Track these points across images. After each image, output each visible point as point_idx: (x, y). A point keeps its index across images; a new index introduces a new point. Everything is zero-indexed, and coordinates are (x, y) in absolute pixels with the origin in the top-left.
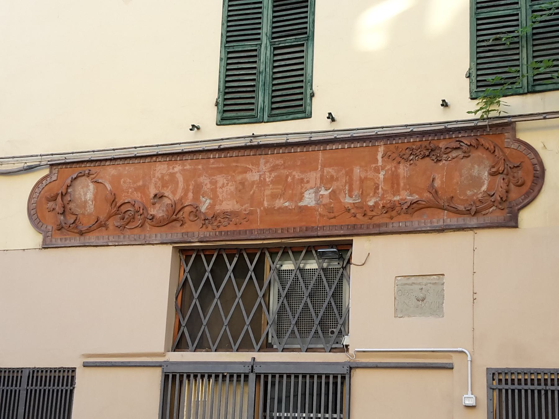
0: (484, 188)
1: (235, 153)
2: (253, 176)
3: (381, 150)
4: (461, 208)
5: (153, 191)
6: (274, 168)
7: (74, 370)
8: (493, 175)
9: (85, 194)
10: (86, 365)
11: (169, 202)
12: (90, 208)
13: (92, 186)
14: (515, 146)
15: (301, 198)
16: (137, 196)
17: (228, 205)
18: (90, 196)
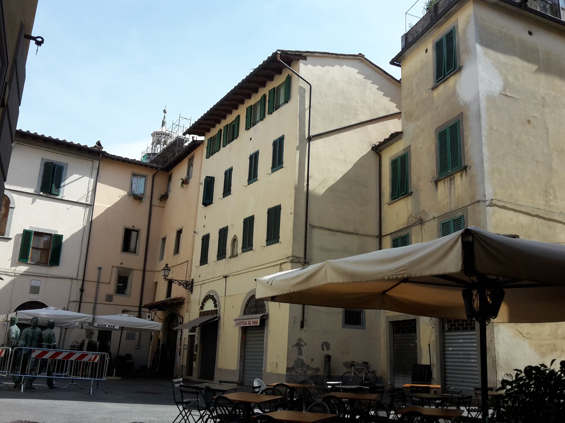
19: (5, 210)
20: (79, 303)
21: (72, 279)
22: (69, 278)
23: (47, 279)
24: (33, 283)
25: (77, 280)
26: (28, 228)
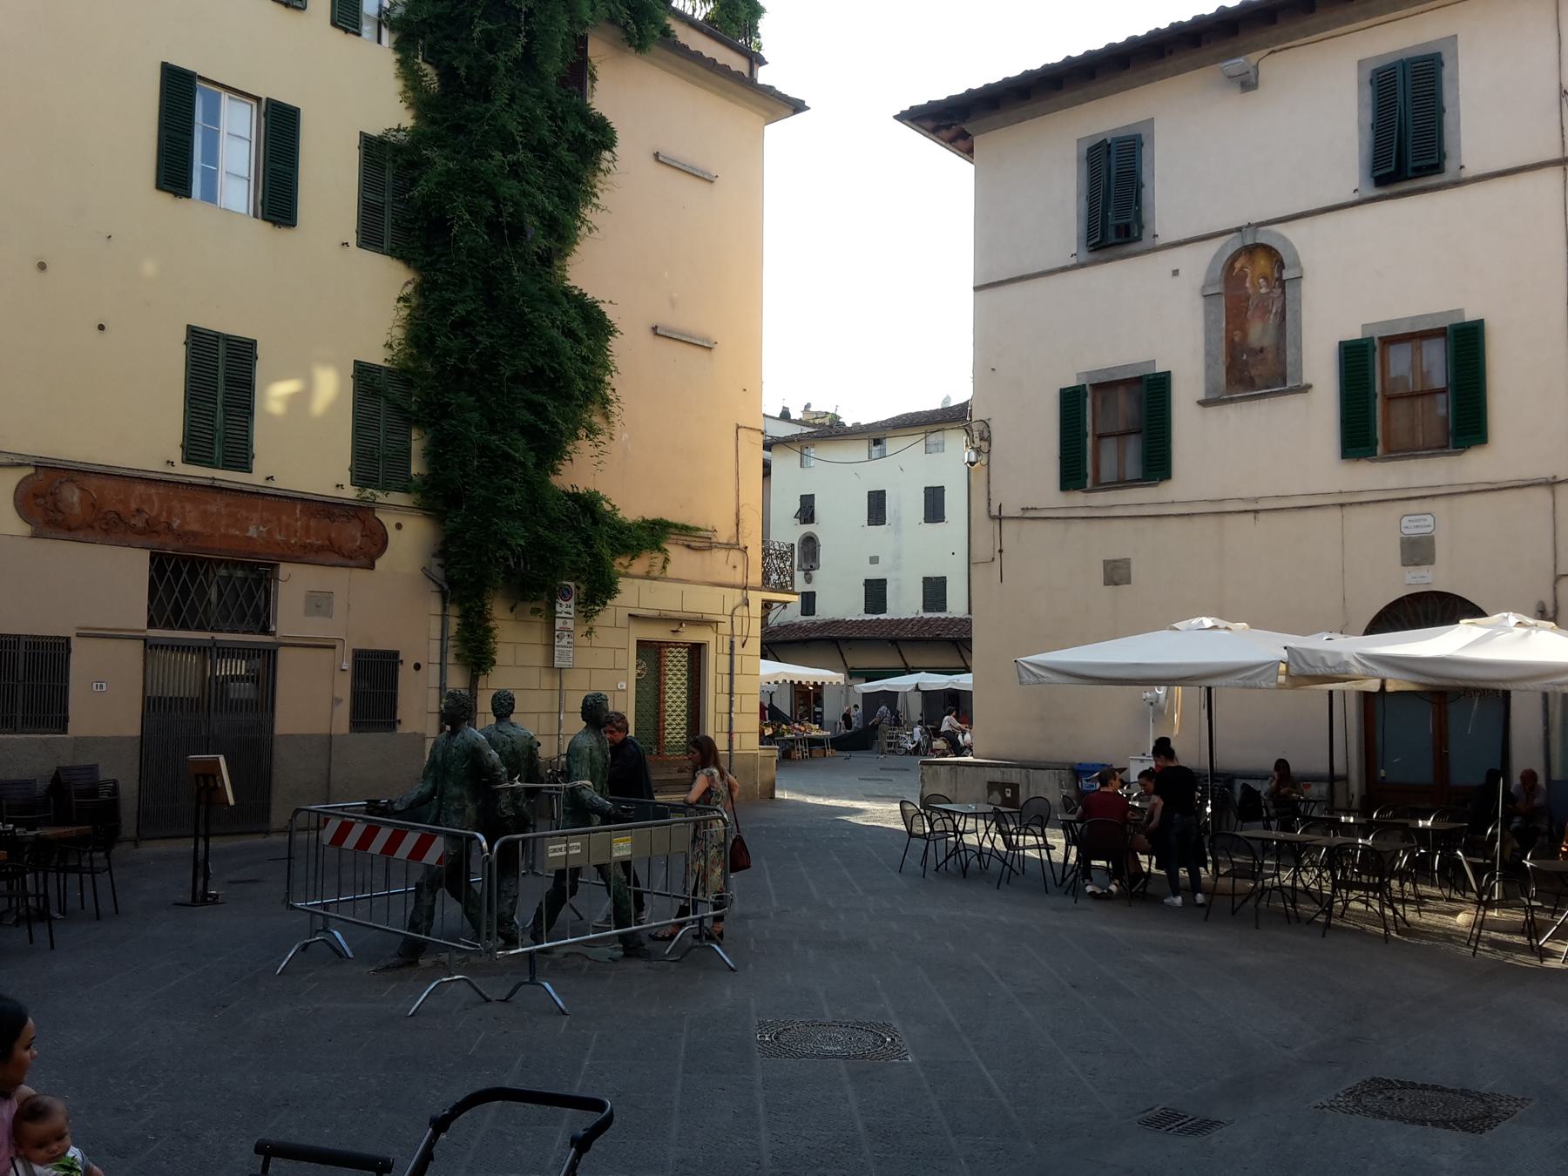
0: (358, 543)
1: (198, 489)
2: (213, 508)
3: (299, 507)
4: (346, 554)
5: (133, 506)
6: (227, 505)
7: (68, 639)
8: (362, 536)
9: (72, 498)
10: (78, 635)
11: (147, 516)
12: (77, 510)
13: (77, 491)
14: (374, 520)
15: (247, 530)
16: (120, 508)
17: (194, 527)
18: (76, 499)
22: (1540, 484)
23: (1457, 501)
24: (1406, 527)
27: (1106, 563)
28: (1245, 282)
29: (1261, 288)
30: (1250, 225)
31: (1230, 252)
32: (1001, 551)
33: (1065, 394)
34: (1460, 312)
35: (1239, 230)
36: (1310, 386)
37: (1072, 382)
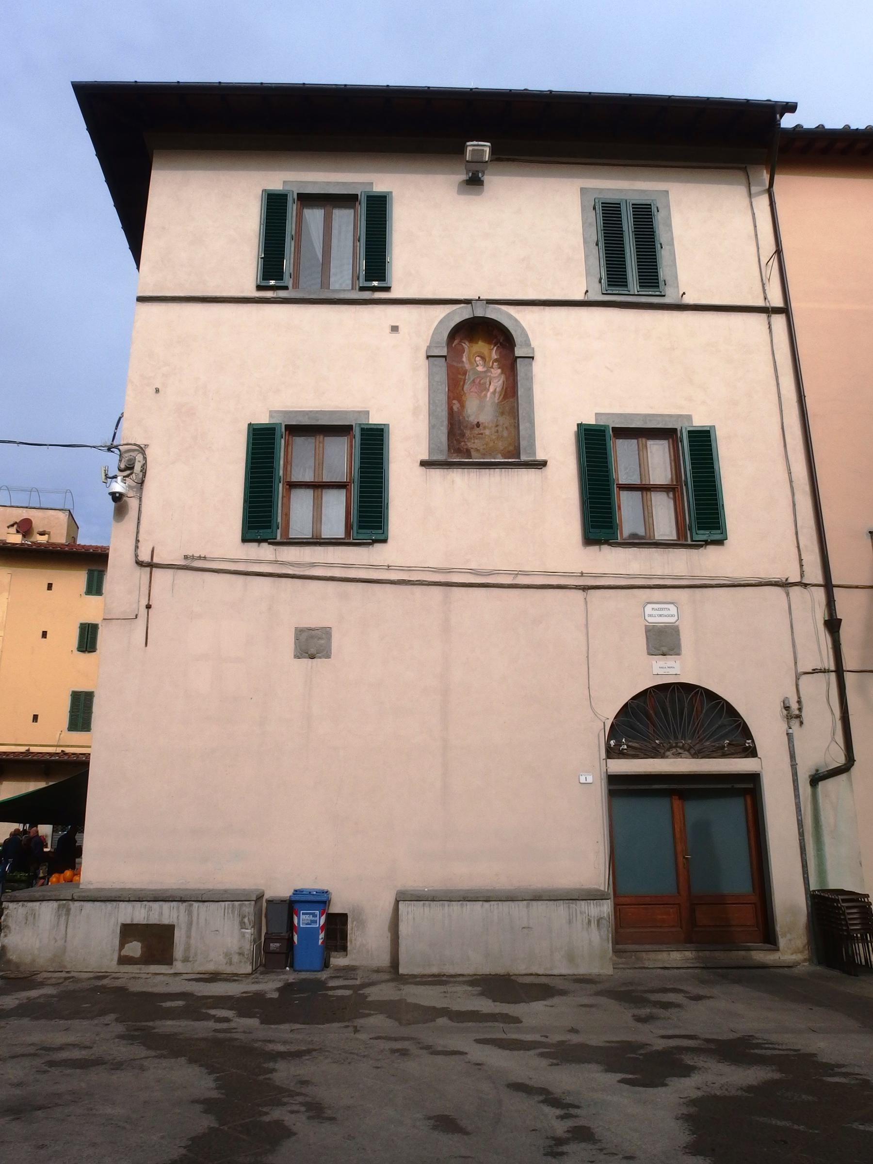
19: (503, 378)
20: (833, 677)
21: (785, 585)
24: (650, 616)
25: (806, 585)
26: (590, 420)
27: (299, 632)
28: (462, 357)
29: (478, 366)
30: (479, 299)
31: (458, 320)
32: (148, 607)
33: (254, 430)
34: (689, 418)
35: (468, 302)
36: (543, 464)
37: (264, 419)
